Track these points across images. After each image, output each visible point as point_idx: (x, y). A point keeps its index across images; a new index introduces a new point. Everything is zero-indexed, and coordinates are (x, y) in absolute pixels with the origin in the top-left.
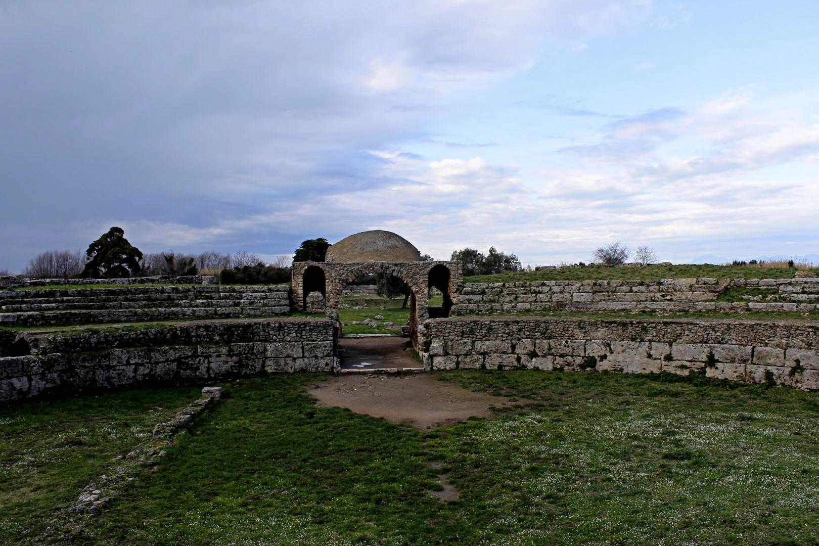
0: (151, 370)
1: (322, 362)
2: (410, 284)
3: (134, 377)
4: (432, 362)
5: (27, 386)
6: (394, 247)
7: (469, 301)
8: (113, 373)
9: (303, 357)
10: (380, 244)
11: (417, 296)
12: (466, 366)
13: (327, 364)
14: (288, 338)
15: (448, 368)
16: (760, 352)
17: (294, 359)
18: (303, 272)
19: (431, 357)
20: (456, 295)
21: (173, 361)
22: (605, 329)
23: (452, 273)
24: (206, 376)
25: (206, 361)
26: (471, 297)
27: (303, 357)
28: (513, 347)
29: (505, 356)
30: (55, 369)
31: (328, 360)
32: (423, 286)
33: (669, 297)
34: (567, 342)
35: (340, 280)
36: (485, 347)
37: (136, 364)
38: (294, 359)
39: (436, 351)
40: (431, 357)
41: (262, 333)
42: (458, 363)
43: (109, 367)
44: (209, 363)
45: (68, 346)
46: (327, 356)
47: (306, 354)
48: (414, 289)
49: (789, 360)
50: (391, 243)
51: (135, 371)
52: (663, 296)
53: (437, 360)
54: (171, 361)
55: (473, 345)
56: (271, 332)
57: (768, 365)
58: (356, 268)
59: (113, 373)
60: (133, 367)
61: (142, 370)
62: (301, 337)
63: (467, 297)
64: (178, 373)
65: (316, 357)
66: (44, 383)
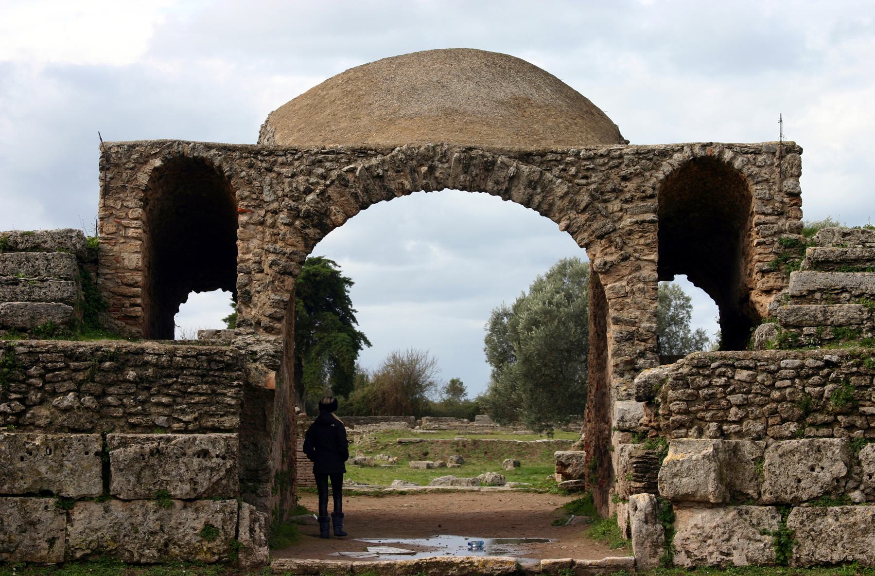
1: (189, 523)
4: (669, 533)
6: (519, 104)
7: (832, 294)
9: (106, 495)
10: (465, 92)
12: (823, 552)
13: (209, 531)
15: (738, 559)
17: (66, 505)
18: (143, 178)
19: (664, 513)
20: (771, 280)
23: (756, 191)
26: (839, 278)
27: (106, 495)
31: (212, 511)
32: (637, 241)
35: (295, 213)
38: (66, 505)
39: (686, 484)
40: (664, 513)
42: (785, 542)
46: (211, 494)
50: (507, 90)
53: (690, 524)
55: (853, 462)
58: (360, 165)
62: (102, 411)
63: (822, 278)
65: (163, 498)
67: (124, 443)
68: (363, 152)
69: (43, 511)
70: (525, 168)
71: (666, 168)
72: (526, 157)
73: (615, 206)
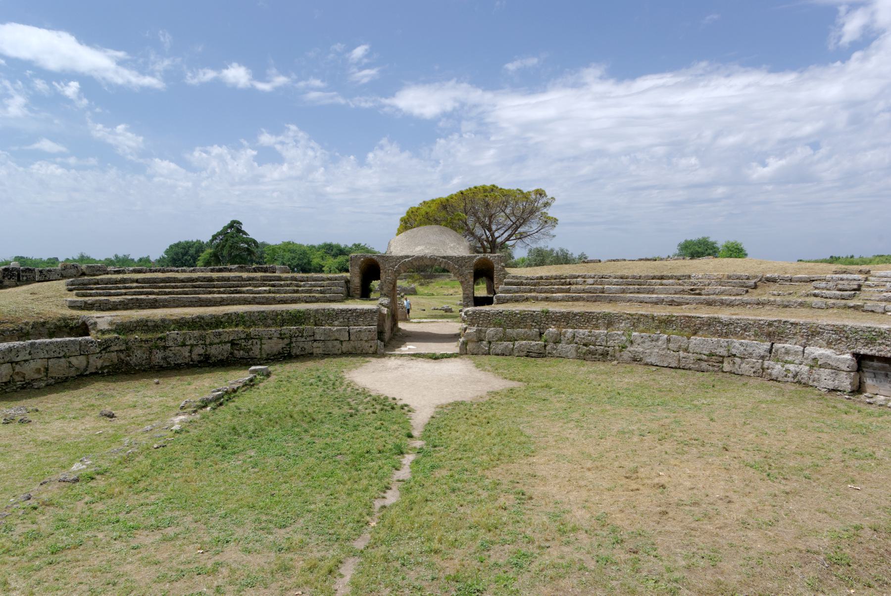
3: (190, 356)
5: (85, 363)
8: (168, 353)
14: (336, 323)
21: (226, 343)
24: (259, 357)
25: (259, 343)
28: (541, 334)
30: (112, 349)
31: (372, 343)
33: (697, 292)
37: (192, 346)
38: (342, 341)
43: (165, 348)
44: (261, 344)
45: (123, 328)
47: (352, 338)
49: (807, 359)
51: (191, 352)
52: (692, 290)
54: (226, 343)
57: (786, 362)
59: (168, 353)
60: (189, 347)
61: (199, 350)
64: (232, 353)
66: (101, 361)
68: (407, 257)
69: (336, 343)
72: (444, 257)
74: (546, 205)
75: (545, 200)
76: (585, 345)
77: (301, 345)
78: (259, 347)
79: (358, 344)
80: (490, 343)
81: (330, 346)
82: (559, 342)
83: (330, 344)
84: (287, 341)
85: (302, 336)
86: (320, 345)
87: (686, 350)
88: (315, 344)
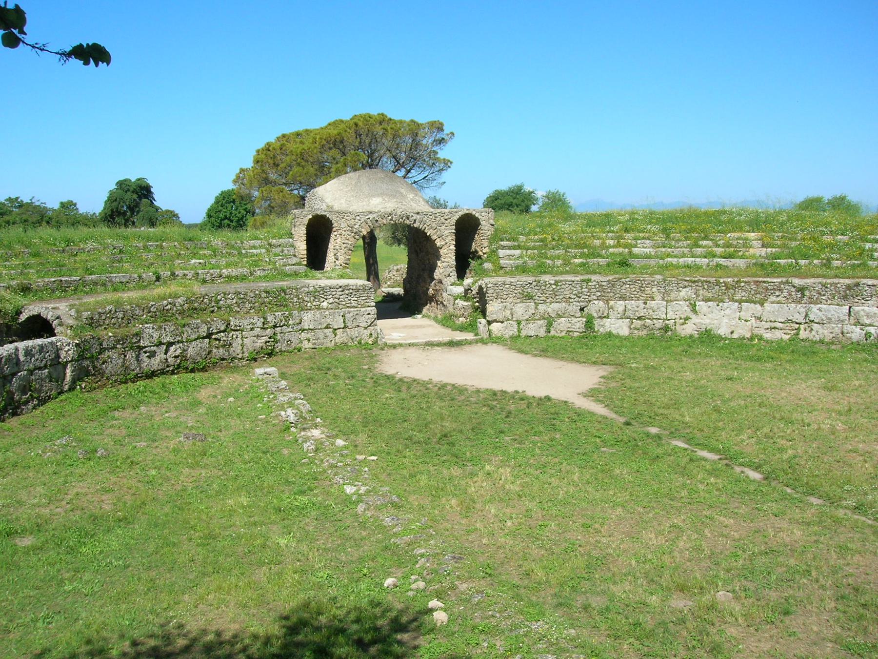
0: (184, 350)
2: (434, 237)
11: (442, 252)
14: (325, 304)
16: (858, 312)
21: (204, 338)
22: (687, 289)
25: (240, 336)
29: (575, 320)
34: (645, 303)
36: (549, 310)
37: (170, 344)
39: (495, 317)
41: (295, 299)
48: (438, 243)
56: (306, 299)
58: (371, 216)
67: (349, 313)
68: (371, 213)
70: (418, 217)
71: (456, 217)
72: (418, 213)
73: (444, 227)
74: (441, 141)
75: (439, 136)
76: (639, 318)
77: (287, 336)
78: (240, 342)
79: (354, 333)
80: (519, 323)
81: (322, 337)
82: (607, 317)
83: (320, 334)
84: (269, 332)
85: (288, 326)
86: (309, 335)
87: (759, 319)
88: (304, 335)
